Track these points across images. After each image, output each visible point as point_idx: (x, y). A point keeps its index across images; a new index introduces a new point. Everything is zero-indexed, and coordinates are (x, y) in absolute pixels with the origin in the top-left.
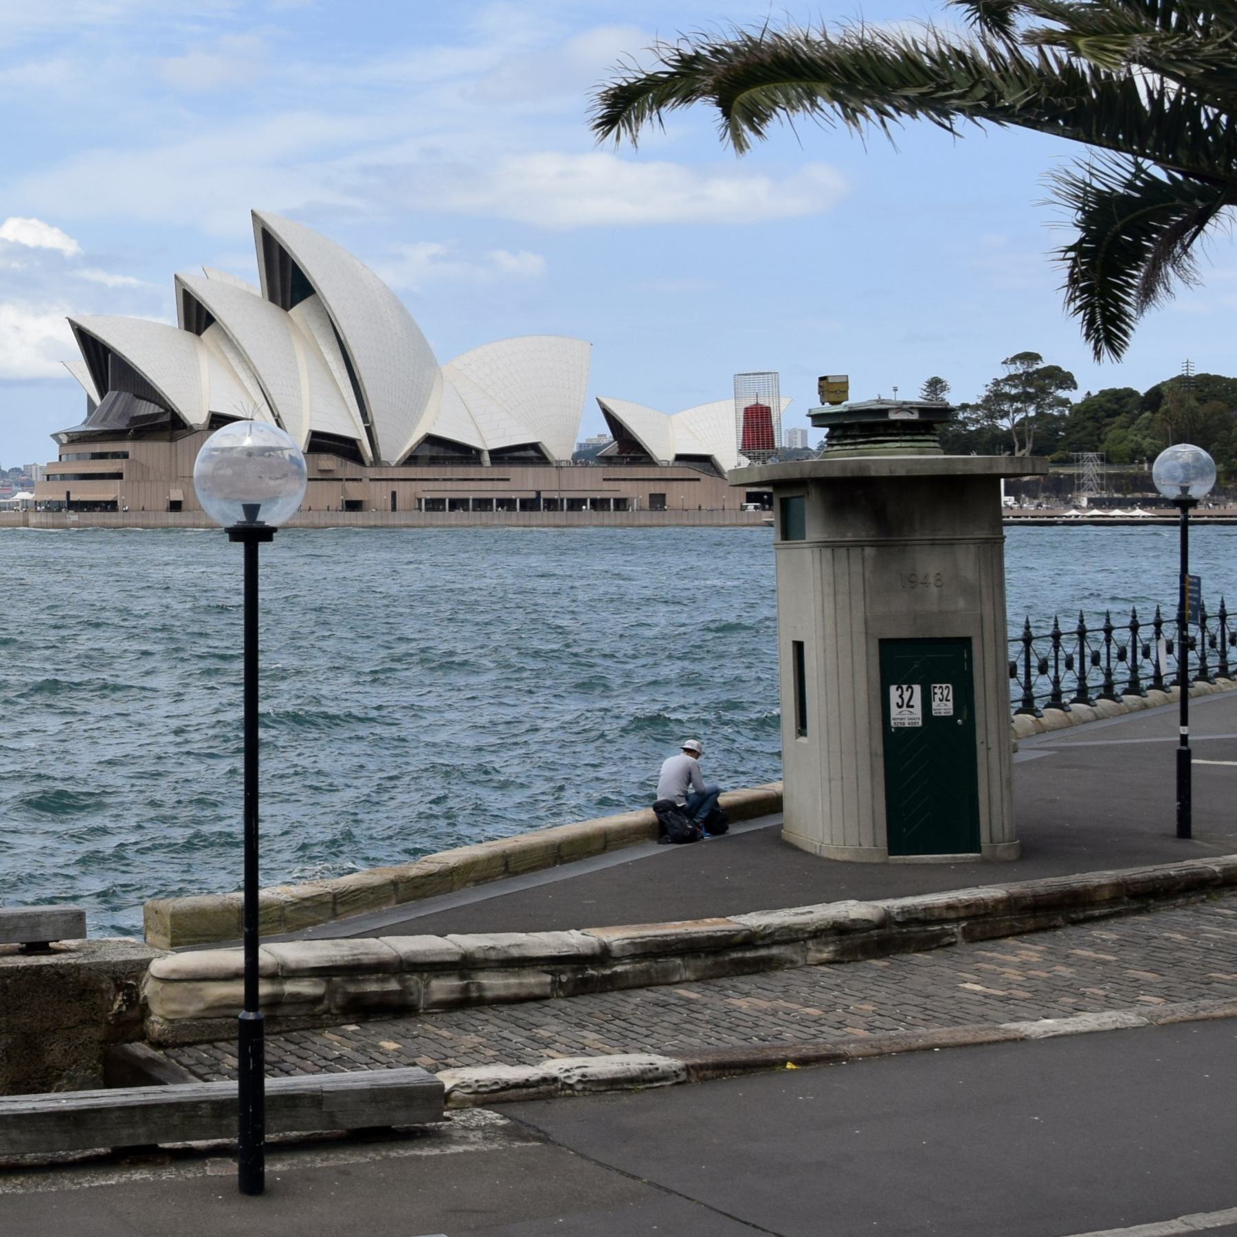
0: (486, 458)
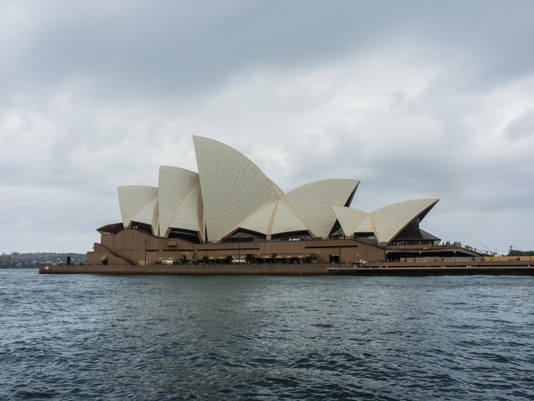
0: (269, 238)
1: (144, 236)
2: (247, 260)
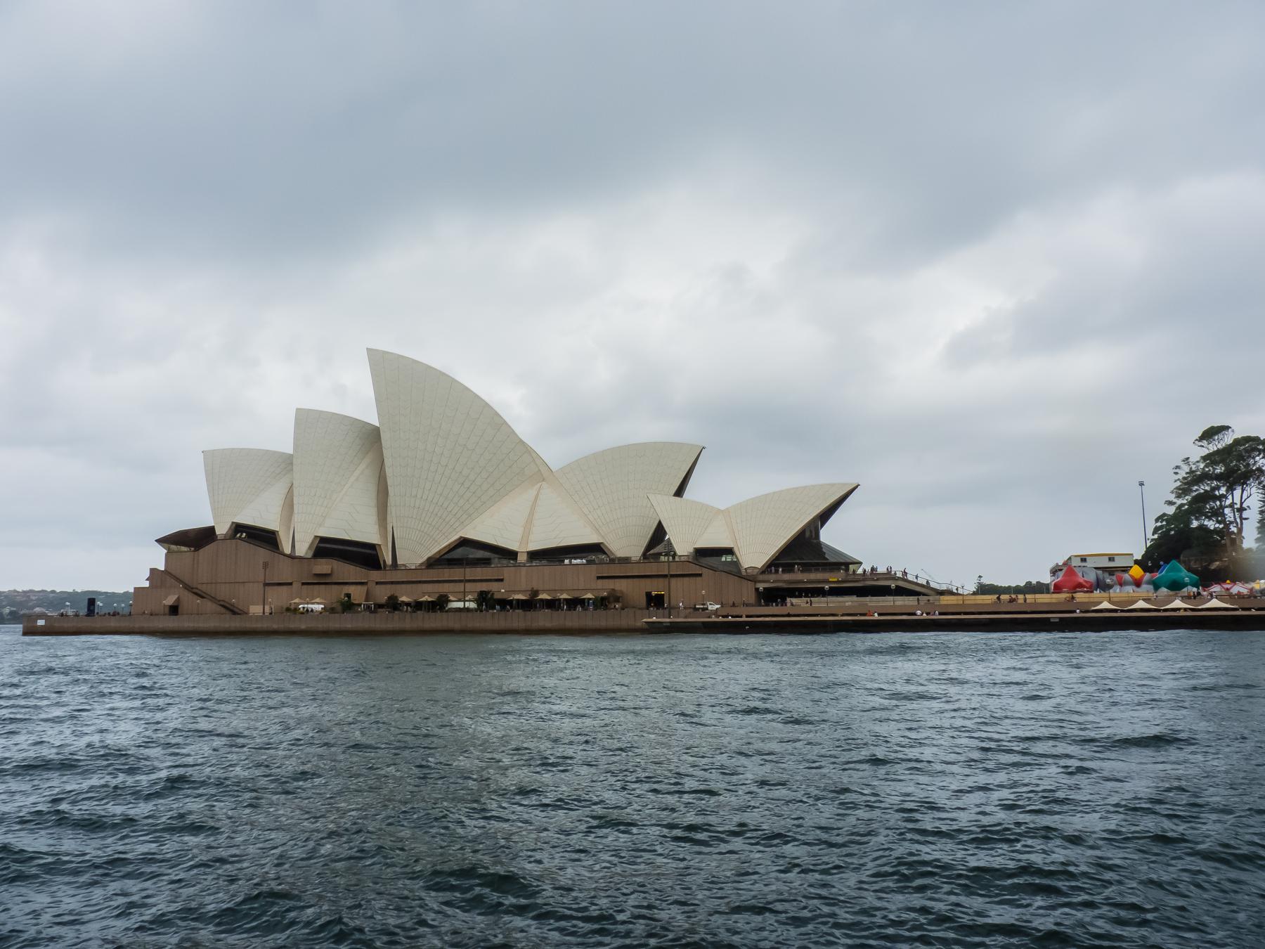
0: (522, 558)
1: (262, 553)
2: (480, 605)
